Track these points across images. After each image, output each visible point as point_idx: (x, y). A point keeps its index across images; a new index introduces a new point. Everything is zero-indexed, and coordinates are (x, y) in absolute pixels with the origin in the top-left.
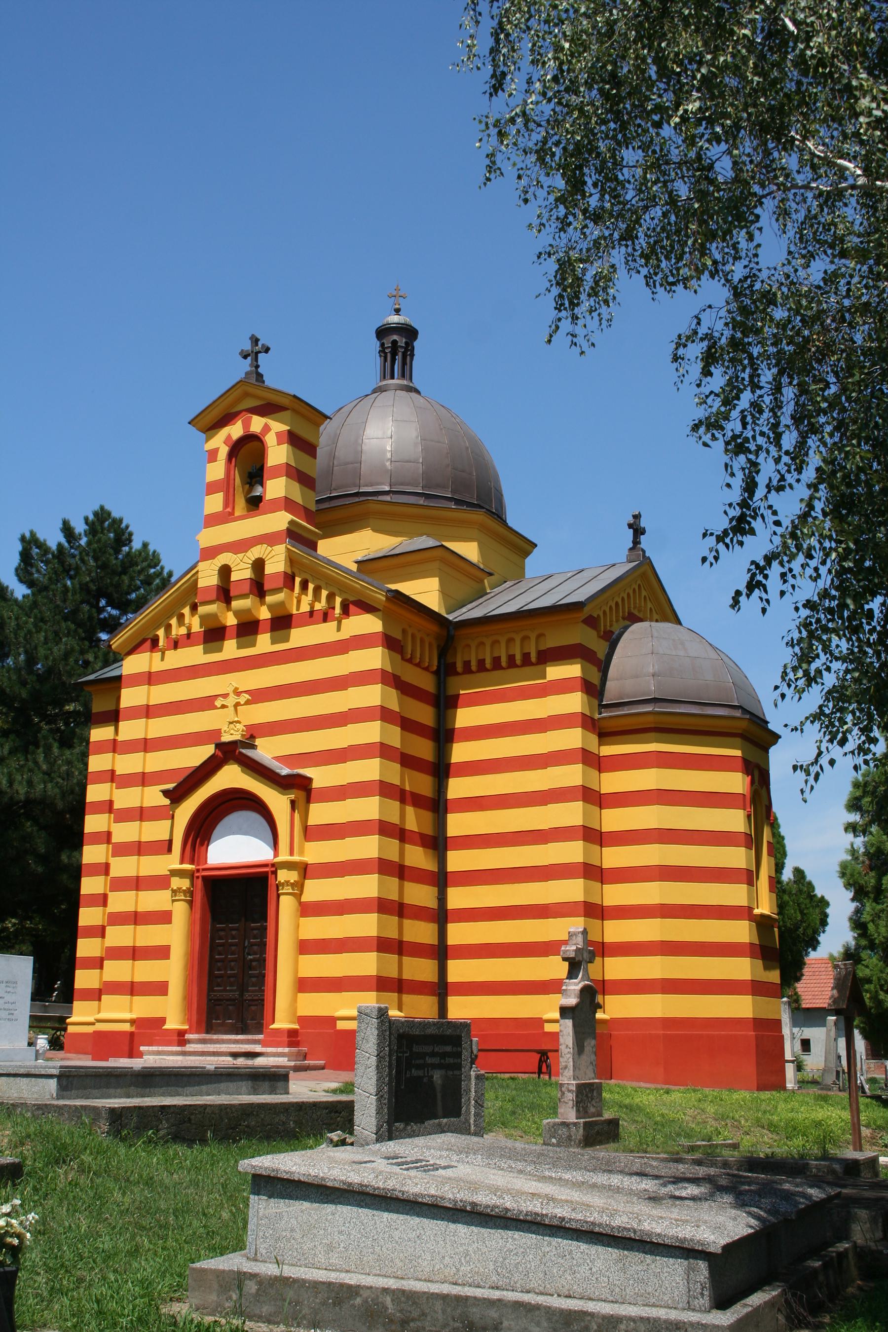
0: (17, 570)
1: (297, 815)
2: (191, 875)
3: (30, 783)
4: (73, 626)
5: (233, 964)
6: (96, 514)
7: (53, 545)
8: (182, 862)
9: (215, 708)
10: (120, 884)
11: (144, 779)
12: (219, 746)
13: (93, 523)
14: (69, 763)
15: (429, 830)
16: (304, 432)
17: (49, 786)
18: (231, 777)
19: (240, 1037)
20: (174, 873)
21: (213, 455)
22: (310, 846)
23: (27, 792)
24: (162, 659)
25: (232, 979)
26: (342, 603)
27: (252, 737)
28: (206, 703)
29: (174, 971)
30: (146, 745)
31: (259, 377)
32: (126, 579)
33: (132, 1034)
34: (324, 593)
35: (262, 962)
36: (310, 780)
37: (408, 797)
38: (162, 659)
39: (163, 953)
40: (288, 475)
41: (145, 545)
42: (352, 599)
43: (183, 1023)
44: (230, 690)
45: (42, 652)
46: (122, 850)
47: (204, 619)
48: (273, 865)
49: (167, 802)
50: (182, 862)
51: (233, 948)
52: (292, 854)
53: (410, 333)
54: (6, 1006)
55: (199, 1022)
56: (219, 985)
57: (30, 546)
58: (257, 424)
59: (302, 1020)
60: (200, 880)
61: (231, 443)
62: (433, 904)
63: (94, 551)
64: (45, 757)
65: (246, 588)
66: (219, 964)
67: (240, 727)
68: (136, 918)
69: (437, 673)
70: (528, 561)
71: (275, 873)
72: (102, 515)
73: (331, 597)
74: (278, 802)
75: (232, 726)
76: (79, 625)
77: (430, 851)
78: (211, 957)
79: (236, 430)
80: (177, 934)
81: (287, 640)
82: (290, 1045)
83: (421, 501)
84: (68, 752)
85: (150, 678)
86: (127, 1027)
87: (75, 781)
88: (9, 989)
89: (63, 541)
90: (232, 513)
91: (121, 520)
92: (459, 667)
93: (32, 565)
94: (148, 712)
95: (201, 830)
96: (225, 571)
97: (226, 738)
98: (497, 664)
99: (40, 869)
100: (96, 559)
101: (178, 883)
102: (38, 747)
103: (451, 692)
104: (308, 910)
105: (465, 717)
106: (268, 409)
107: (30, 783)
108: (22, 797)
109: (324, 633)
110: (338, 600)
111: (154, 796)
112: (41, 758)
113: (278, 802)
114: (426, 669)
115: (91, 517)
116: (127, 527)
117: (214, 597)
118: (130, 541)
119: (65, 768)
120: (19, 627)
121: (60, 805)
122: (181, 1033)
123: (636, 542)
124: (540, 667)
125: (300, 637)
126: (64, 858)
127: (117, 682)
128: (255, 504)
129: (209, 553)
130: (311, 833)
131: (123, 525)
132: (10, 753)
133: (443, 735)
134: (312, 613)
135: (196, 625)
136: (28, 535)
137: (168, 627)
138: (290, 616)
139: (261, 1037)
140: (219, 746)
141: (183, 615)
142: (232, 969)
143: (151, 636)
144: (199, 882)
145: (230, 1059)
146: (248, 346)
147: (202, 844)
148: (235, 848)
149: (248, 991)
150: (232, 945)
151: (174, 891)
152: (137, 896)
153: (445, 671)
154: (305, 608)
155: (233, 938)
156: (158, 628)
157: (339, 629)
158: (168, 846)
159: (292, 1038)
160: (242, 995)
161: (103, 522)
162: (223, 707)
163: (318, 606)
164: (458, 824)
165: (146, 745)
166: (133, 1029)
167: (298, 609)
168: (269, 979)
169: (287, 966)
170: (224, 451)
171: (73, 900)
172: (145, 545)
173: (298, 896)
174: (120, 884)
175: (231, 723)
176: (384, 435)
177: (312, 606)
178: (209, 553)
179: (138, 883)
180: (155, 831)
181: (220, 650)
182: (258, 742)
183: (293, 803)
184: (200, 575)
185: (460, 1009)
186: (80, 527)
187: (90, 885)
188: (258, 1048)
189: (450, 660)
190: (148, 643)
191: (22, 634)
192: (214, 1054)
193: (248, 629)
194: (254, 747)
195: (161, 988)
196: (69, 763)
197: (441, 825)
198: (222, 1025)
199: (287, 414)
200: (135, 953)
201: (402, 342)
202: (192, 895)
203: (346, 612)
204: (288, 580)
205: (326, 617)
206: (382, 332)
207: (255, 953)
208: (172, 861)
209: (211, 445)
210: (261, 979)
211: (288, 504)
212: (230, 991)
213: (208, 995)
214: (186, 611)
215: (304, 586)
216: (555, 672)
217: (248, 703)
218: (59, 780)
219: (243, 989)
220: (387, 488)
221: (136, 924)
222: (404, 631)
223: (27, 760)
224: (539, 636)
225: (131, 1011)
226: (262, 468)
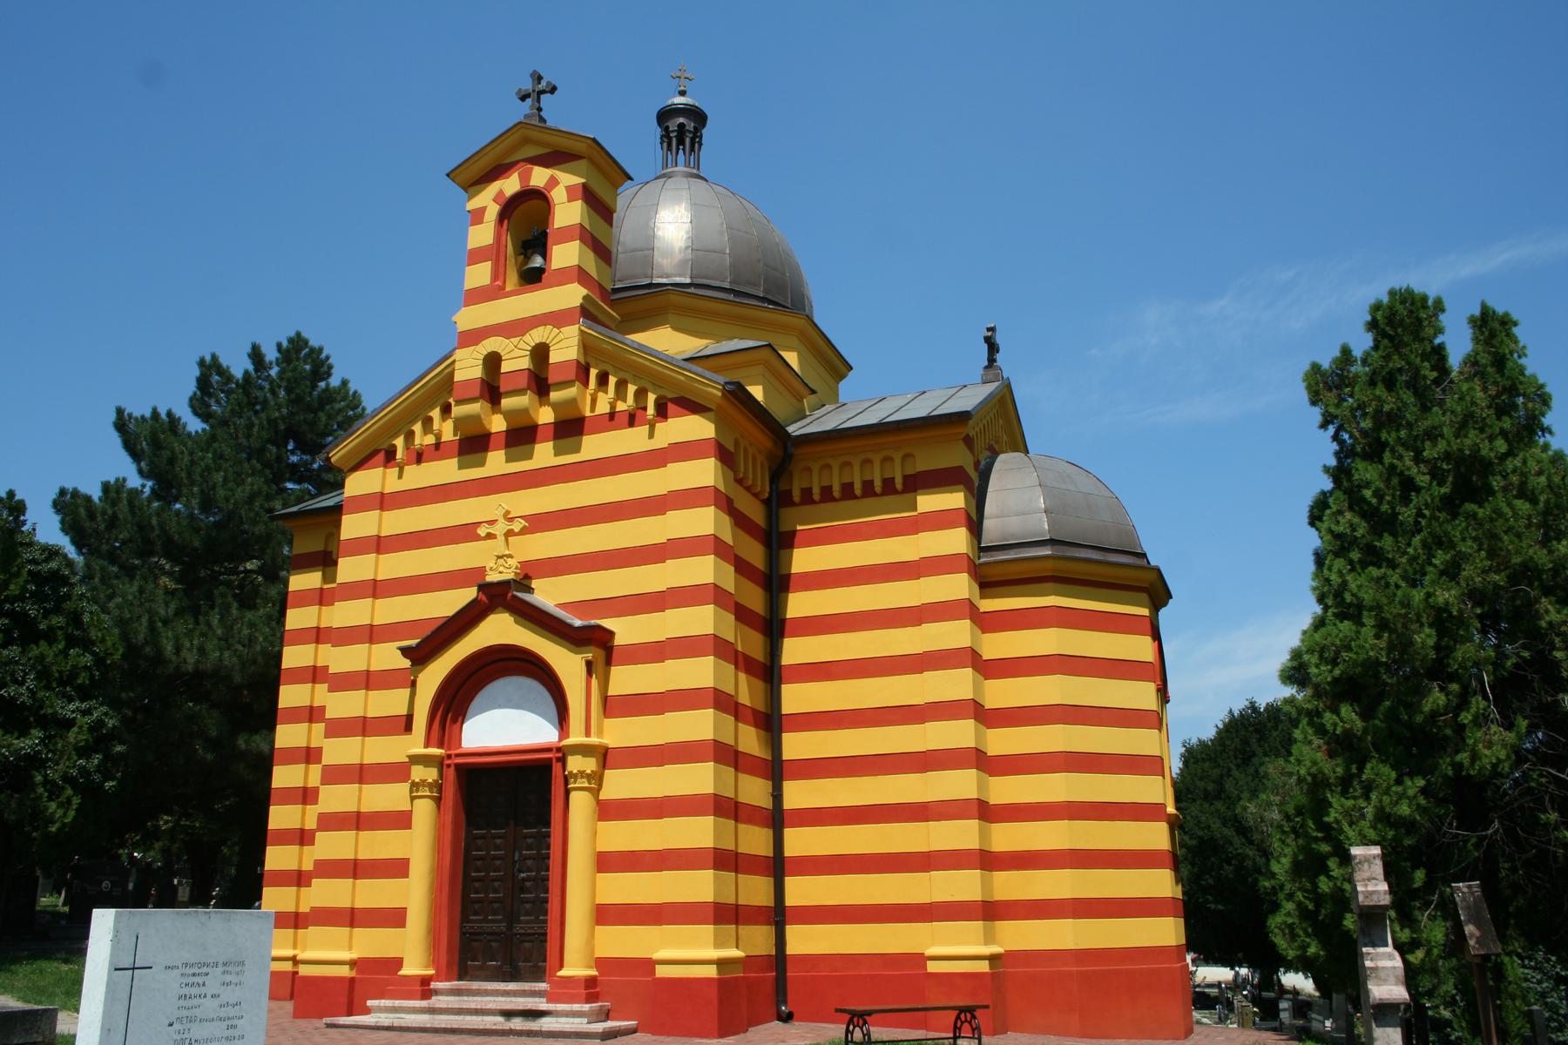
0: (191, 400)
1: (594, 681)
2: (440, 763)
3: (202, 650)
4: (259, 466)
5: (497, 884)
6: (291, 340)
7: (238, 373)
8: (427, 745)
9: (478, 538)
10: (336, 775)
11: (372, 634)
12: (484, 588)
13: (288, 350)
14: (252, 625)
15: (761, 707)
16: (600, 189)
17: (227, 654)
18: (499, 629)
19: (512, 986)
20: (416, 759)
21: (477, 216)
22: (611, 723)
23: (198, 661)
24: (400, 477)
25: (496, 905)
26: (656, 402)
27: (527, 577)
28: (465, 533)
29: (414, 893)
30: (376, 589)
31: (542, 120)
32: (323, 416)
33: (352, 980)
34: (632, 389)
35: (542, 883)
36: (611, 634)
37: (740, 658)
38: (400, 477)
39: (397, 868)
40: (582, 239)
41: (345, 383)
42: (670, 395)
43: (427, 967)
44: (498, 514)
45: (221, 493)
46: (340, 728)
47: (459, 424)
48: (559, 749)
49: (407, 663)
50: (427, 745)
51: (498, 862)
52: (588, 734)
53: (698, 116)
54: (223, 1013)
55: (449, 965)
56: (476, 914)
57: (210, 371)
58: (539, 176)
59: (601, 963)
61: (503, 201)
62: (765, 802)
63: (288, 380)
64: (220, 620)
65: (523, 381)
66: (477, 884)
67: (513, 562)
68: (359, 821)
69: (767, 503)
70: (842, 385)
71: (563, 760)
72: (298, 342)
73: (641, 394)
74: (568, 664)
75: (501, 561)
76: (267, 465)
77: (762, 733)
78: (466, 874)
79: (510, 185)
80: (418, 844)
81: (577, 450)
82: (590, 998)
83: (731, 297)
84: (249, 615)
85: (383, 501)
86: (345, 971)
87: (258, 648)
88: (228, 978)
89: (251, 368)
90: (503, 288)
91: (321, 350)
92: (797, 497)
93: (210, 396)
94: (380, 545)
95: (454, 702)
96: (493, 361)
97: (492, 577)
98: (848, 492)
99: (209, 757)
100: (289, 391)
101: (418, 773)
102: (212, 607)
103: (785, 528)
104: (608, 811)
105: (803, 560)
106: (555, 158)
107: (202, 650)
108: (190, 668)
109: (633, 440)
110: (651, 398)
111: (388, 656)
112: (215, 621)
113: (568, 664)
114: (756, 495)
115: (285, 344)
116: (328, 358)
117: (477, 392)
118: (329, 375)
119: (246, 632)
120: (193, 462)
121: (238, 678)
122: (425, 981)
123: (992, 360)
125: (594, 446)
126: (241, 743)
127: (337, 511)
128: (532, 278)
129: (471, 338)
130: (614, 706)
131: (323, 356)
132: (176, 614)
133: (777, 583)
134: (612, 415)
135: (448, 432)
136: (208, 358)
137: (410, 435)
139: (543, 986)
140: (484, 588)
141: (431, 419)
142: (496, 891)
143: (385, 446)
145: (500, 1019)
146: (528, 85)
147: (454, 721)
148: (502, 727)
149: (519, 922)
150: (495, 858)
151: (415, 786)
152: (360, 790)
153: (777, 501)
154: (603, 407)
155: (498, 848)
156: (396, 436)
157: (651, 436)
158: (407, 724)
159: (590, 989)
160: (510, 927)
161: (298, 351)
162: (490, 536)
163: (621, 406)
164: (795, 698)
165: (376, 589)
166: (353, 974)
167: (593, 409)
168: (554, 905)
170: (493, 211)
171: (259, 797)
172: (345, 383)
173: (595, 792)
174: (336, 775)
175: (499, 557)
176: (672, 225)
177: (613, 406)
178: (471, 338)
179: (361, 774)
180: (390, 702)
181: (482, 464)
182: (535, 584)
183: (589, 664)
184: (457, 365)
185: (802, 940)
186: (271, 354)
187: (284, 776)
188: (543, 1005)
189: (783, 487)
190: (381, 456)
191: (199, 470)
192: (477, 1012)
193: (522, 436)
194: (530, 590)
195: (396, 918)
196: (252, 625)
197: (774, 698)
198: (481, 968)
199: (582, 164)
200: (356, 869)
201: (690, 126)
202: (440, 789)
203: (662, 412)
204: (582, 372)
205: (632, 420)
206: (664, 115)
207: (530, 870)
208: (415, 744)
209: (474, 204)
210: (541, 906)
211: (581, 275)
213: (462, 927)
214: (436, 413)
215: (603, 381)
216: (928, 502)
217: (524, 531)
218: (240, 647)
219: (512, 919)
220: (688, 281)
221: (358, 828)
222: (737, 443)
223: (197, 623)
224: (906, 457)
225: (350, 949)
226: (545, 235)
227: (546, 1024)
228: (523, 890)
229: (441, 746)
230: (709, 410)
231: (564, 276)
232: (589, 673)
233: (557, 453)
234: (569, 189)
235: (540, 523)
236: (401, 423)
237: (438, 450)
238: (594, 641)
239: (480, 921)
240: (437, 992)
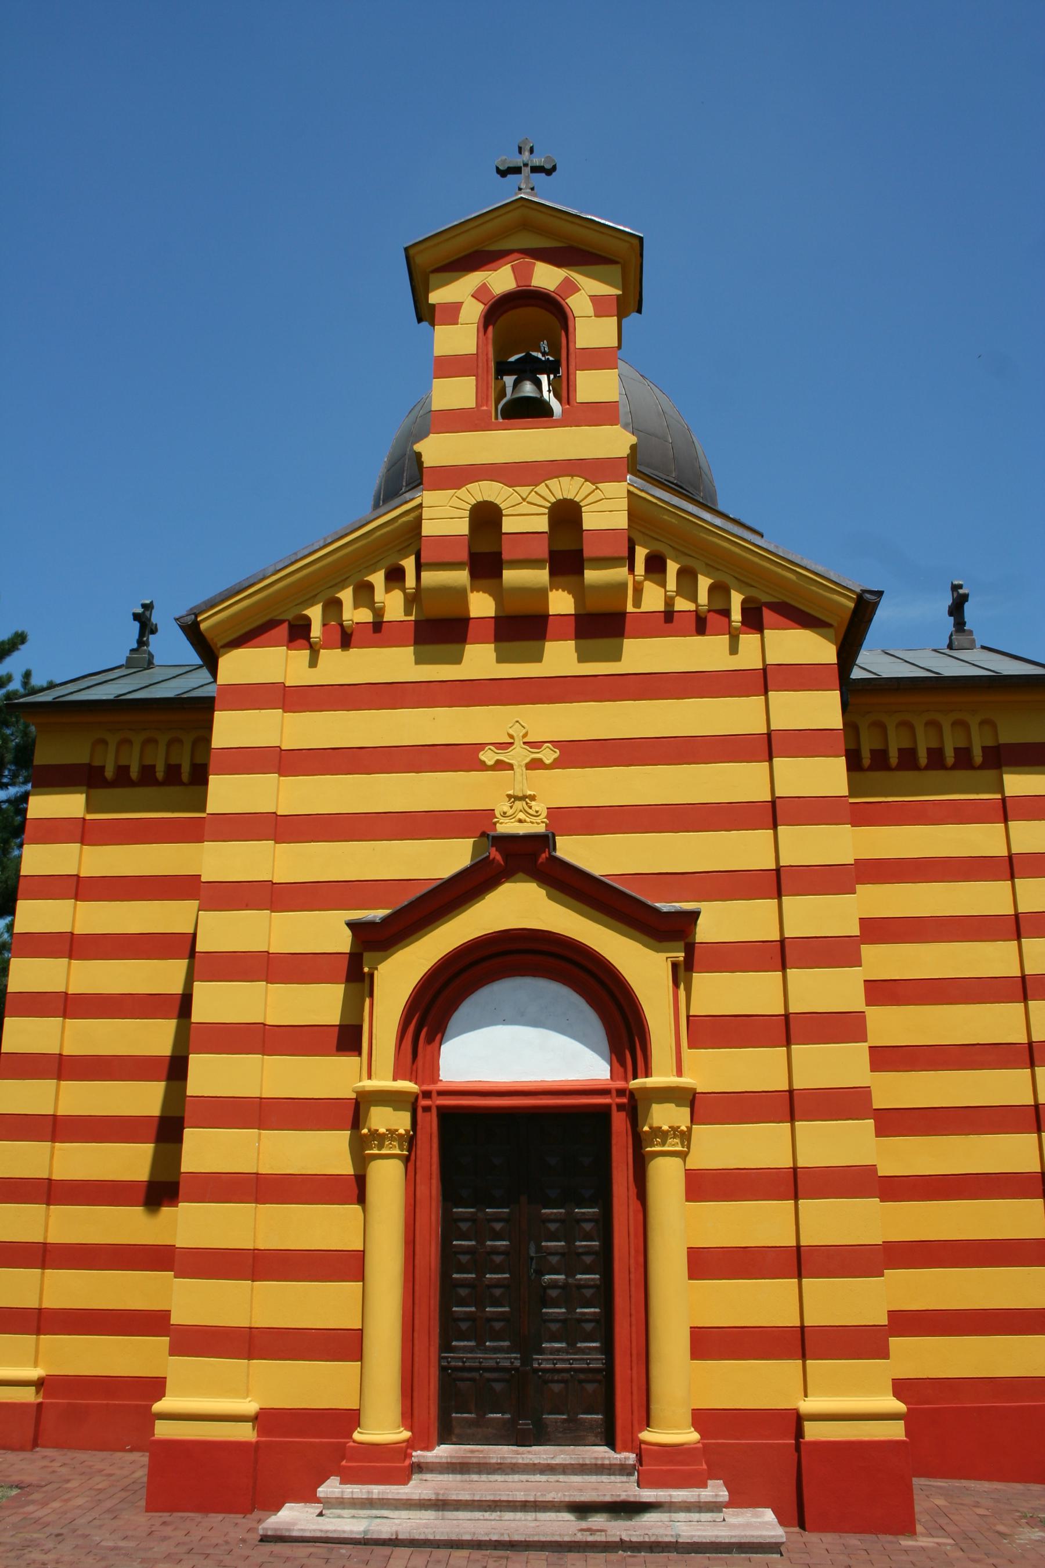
2: (412, 1104)
9: (483, 767)
18: (519, 906)
26: (743, 602)
28: (460, 757)
34: (704, 583)
42: (765, 598)
47: (412, 600)
52: (679, 1073)
58: (546, 277)
60: (434, 1111)
67: (539, 806)
73: (719, 590)
74: (642, 967)
75: (519, 804)
79: (501, 280)
81: (616, 656)
86: (246, 1433)
95: (432, 1013)
97: (506, 827)
98: (908, 760)
106: (577, 251)
109: (708, 653)
110: (736, 599)
113: (642, 967)
117: (464, 555)
122: (402, 1450)
124: (990, 774)
125: (639, 655)
129: (455, 477)
134: (669, 614)
135: (393, 606)
137: (333, 606)
138: (622, 615)
143: (289, 616)
144: (430, 1123)
147: (430, 1040)
148: (519, 1051)
149: (541, 1351)
156: (310, 602)
160: (526, 1360)
169: (679, 1304)
170: (473, 311)
177: (669, 602)
178: (455, 477)
181: (457, 660)
183: (675, 966)
184: (426, 513)
190: (283, 630)
193: (522, 628)
203: (754, 620)
205: (700, 626)
212: (495, 1350)
214: (378, 579)
215: (656, 566)
217: (557, 764)
227: (649, 1526)
228: (546, 1302)
229: (413, 1077)
230: (827, 625)
231: (601, 414)
232: (676, 984)
234: (595, 299)
235: (577, 754)
236: (322, 585)
237: (379, 631)
238: (670, 930)
239: (471, 1350)
240: (420, 1468)
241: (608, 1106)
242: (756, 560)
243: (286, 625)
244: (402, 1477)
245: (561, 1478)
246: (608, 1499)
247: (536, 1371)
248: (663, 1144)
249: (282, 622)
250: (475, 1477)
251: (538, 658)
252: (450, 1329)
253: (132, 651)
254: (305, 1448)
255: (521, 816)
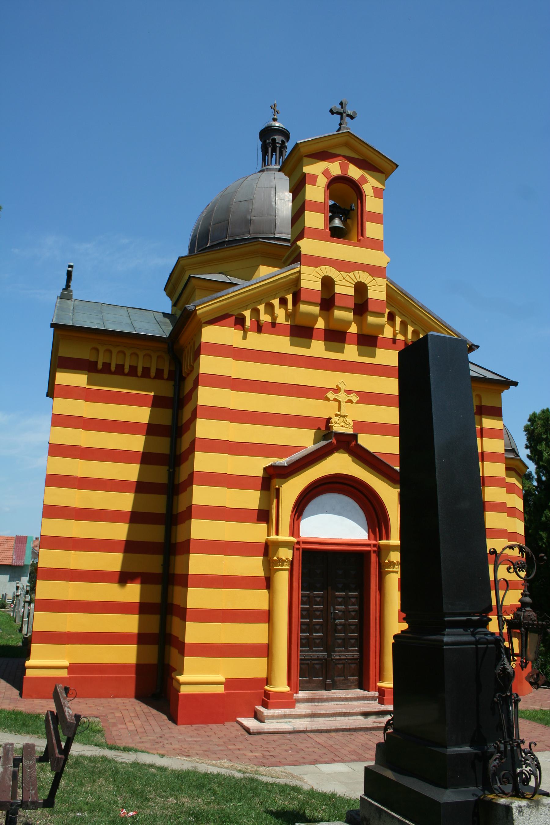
9: (328, 399)
18: (340, 464)
28: (319, 393)
34: (410, 329)
58: (354, 172)
65: (351, 304)
67: (349, 420)
75: (342, 419)
79: (335, 168)
86: (220, 689)
129: (316, 261)
137: (256, 312)
143: (235, 313)
149: (335, 652)
154: (388, 332)
160: (329, 655)
170: (322, 181)
178: (316, 261)
184: (303, 277)
198: (309, 682)
231: (376, 245)
233: (360, 354)
239: (307, 651)
241: (369, 552)
242: (433, 323)
243: (234, 317)
244: (292, 705)
245: (350, 703)
246: (377, 710)
247: (332, 660)
248: (393, 568)
249: (231, 316)
250: (316, 704)
251: (342, 351)
252: (306, 643)
253: (63, 289)
254: (252, 696)
255: (343, 424)
